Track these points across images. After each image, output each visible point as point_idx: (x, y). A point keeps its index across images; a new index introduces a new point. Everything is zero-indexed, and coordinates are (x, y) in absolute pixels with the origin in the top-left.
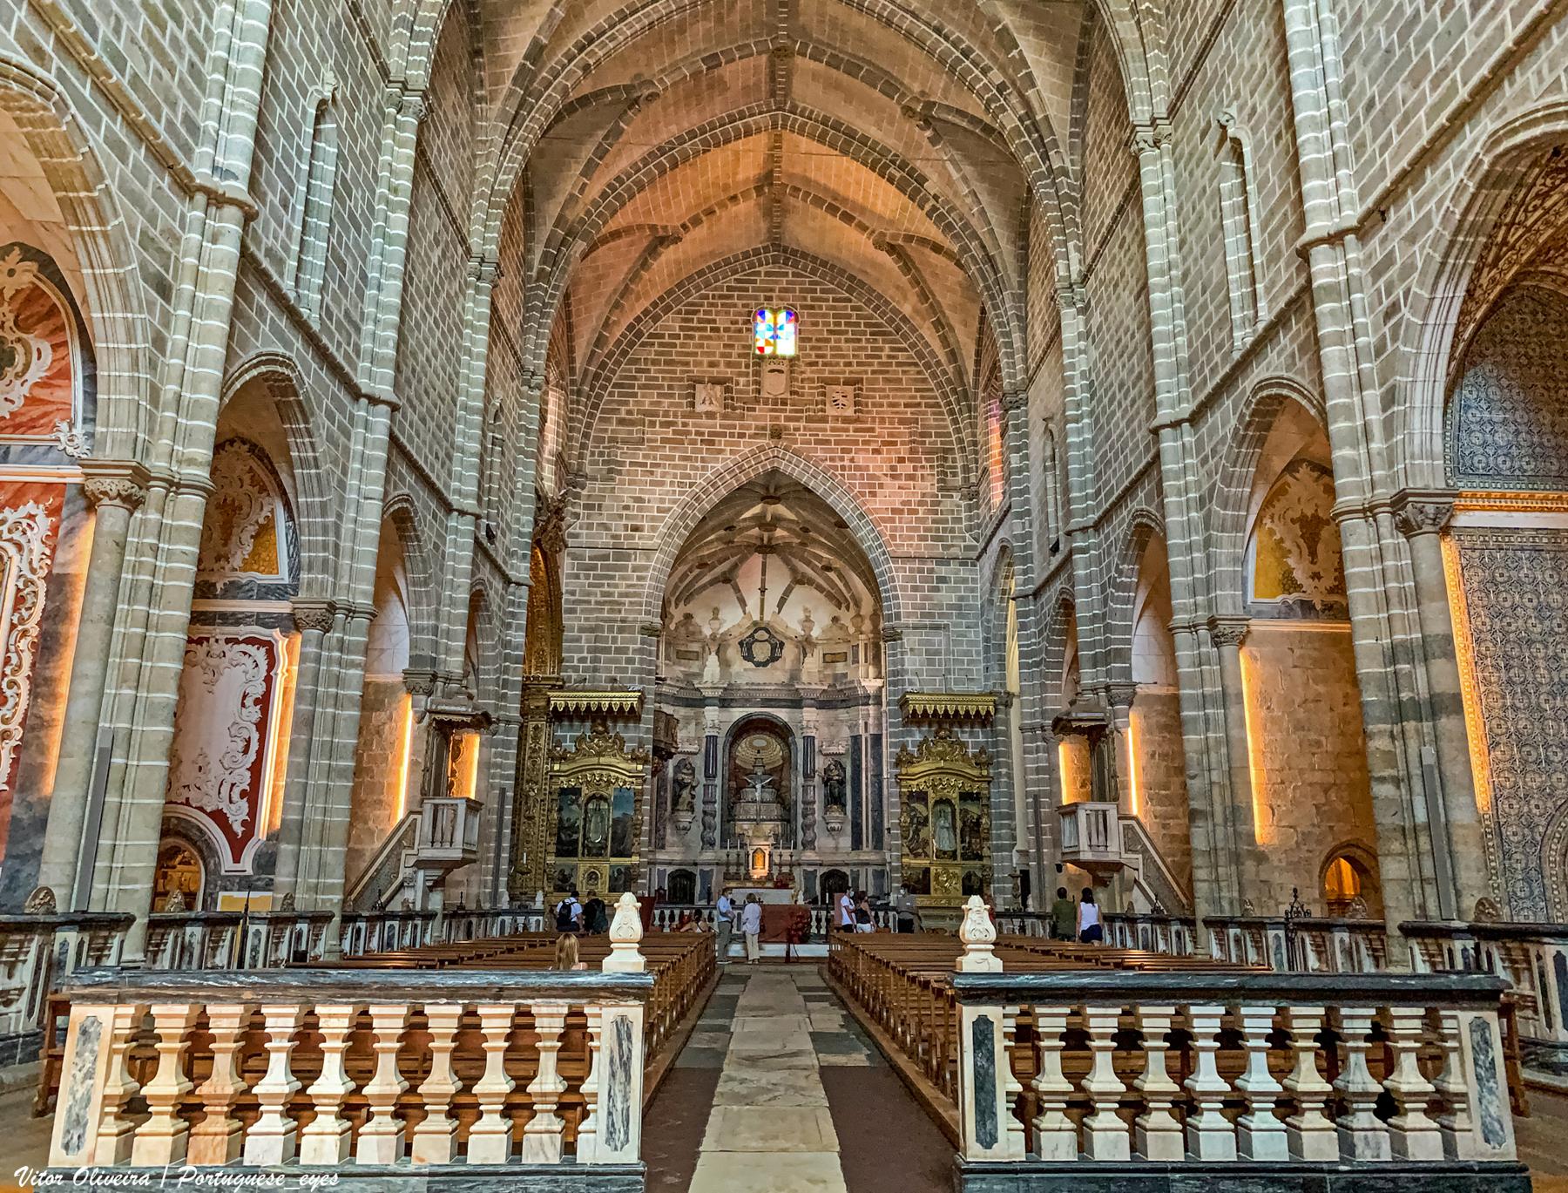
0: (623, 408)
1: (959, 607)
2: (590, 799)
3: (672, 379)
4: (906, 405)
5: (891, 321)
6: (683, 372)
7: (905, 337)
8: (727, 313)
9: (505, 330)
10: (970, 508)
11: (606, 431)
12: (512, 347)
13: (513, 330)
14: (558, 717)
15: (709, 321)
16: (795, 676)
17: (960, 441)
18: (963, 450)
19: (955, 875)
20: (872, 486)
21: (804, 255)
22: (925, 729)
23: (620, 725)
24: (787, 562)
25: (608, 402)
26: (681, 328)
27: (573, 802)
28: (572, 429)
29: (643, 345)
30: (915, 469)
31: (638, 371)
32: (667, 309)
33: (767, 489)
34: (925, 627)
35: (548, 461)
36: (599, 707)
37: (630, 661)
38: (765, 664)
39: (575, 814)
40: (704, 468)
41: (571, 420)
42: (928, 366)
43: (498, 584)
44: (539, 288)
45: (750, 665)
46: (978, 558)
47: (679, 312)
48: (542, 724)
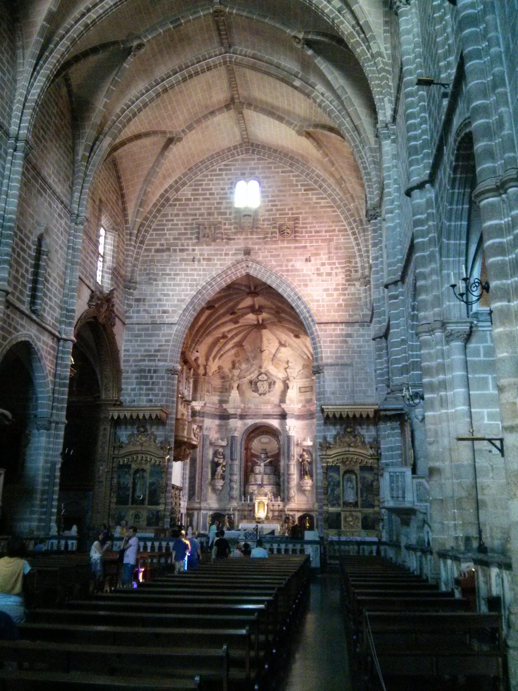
0: (158, 243)
1: (360, 352)
2: (137, 471)
3: (187, 224)
4: (326, 232)
5: (316, 182)
6: (193, 219)
7: (325, 191)
8: (219, 184)
9: (50, 188)
10: (365, 291)
11: (148, 256)
12: (58, 198)
13: (59, 189)
14: (117, 423)
15: (208, 190)
16: (283, 400)
17: (360, 250)
18: (361, 256)
19: (357, 518)
20: (306, 280)
21: (264, 147)
22: (338, 427)
23: (154, 428)
24: (275, 335)
25: (149, 240)
26: (192, 195)
27: (126, 473)
28: (127, 256)
29: (171, 205)
30: (332, 269)
31: (167, 221)
32: (184, 184)
33: (250, 287)
34: (337, 365)
35: (107, 273)
36: (138, 417)
37: (161, 389)
38: (264, 394)
39: (128, 480)
40: (205, 275)
41: (127, 250)
42: (339, 207)
43: (46, 338)
44: (82, 165)
45: (256, 394)
46: (371, 321)
47: (191, 186)
48: (108, 427)
